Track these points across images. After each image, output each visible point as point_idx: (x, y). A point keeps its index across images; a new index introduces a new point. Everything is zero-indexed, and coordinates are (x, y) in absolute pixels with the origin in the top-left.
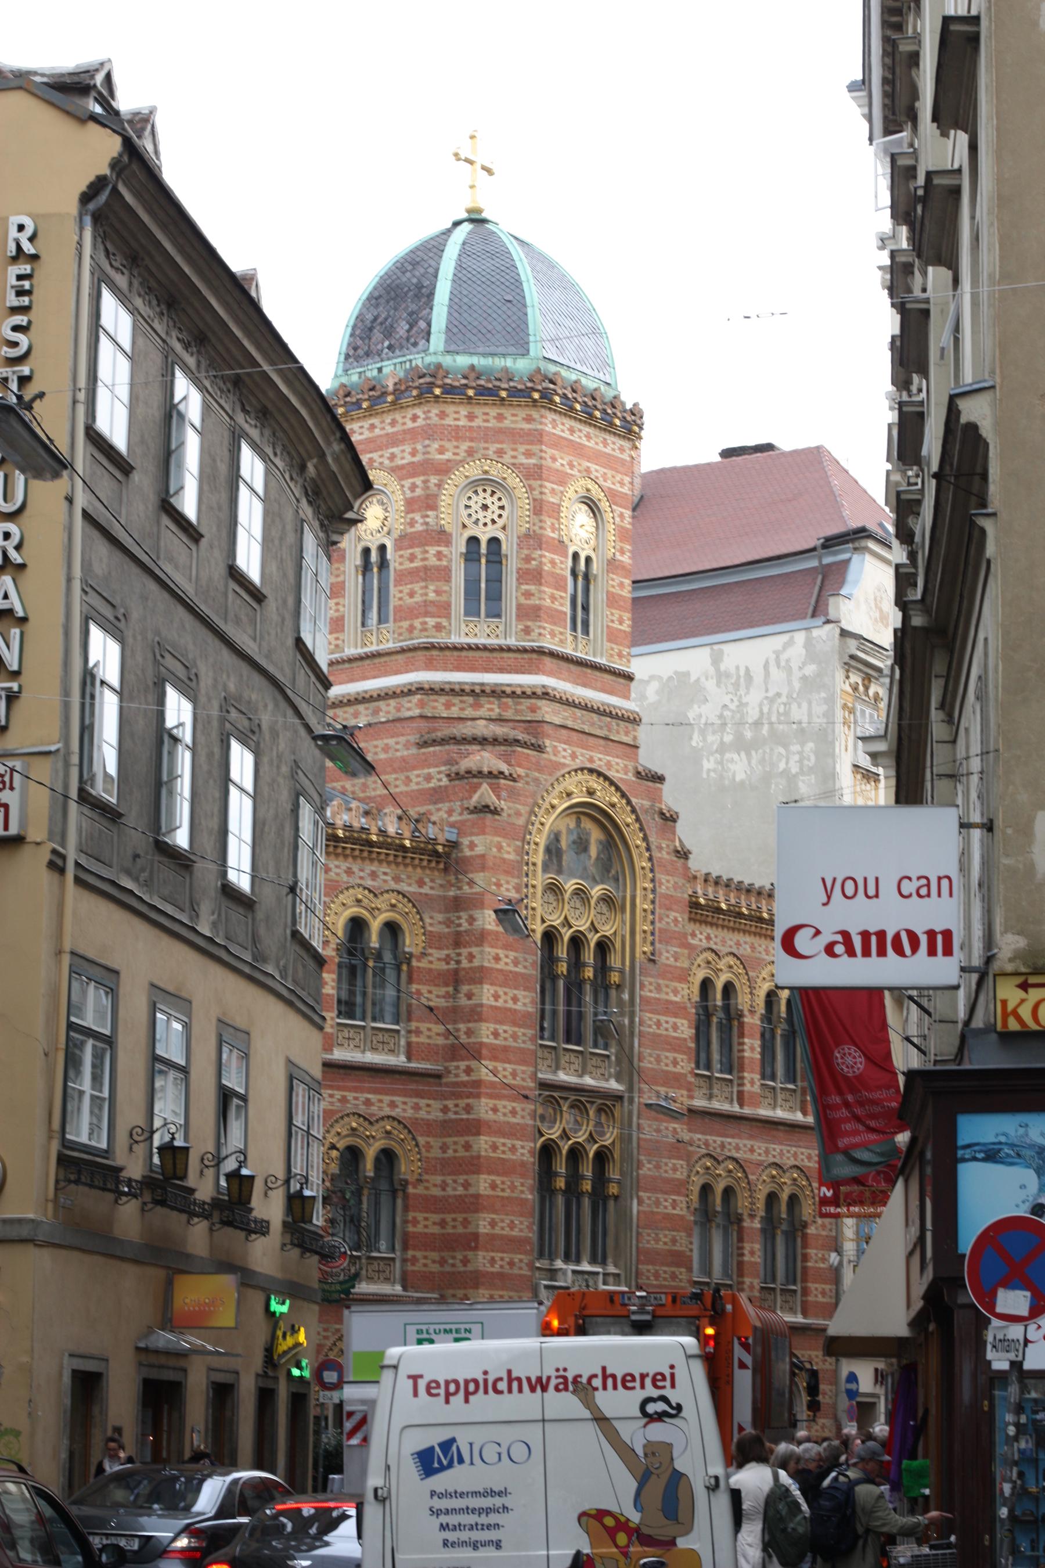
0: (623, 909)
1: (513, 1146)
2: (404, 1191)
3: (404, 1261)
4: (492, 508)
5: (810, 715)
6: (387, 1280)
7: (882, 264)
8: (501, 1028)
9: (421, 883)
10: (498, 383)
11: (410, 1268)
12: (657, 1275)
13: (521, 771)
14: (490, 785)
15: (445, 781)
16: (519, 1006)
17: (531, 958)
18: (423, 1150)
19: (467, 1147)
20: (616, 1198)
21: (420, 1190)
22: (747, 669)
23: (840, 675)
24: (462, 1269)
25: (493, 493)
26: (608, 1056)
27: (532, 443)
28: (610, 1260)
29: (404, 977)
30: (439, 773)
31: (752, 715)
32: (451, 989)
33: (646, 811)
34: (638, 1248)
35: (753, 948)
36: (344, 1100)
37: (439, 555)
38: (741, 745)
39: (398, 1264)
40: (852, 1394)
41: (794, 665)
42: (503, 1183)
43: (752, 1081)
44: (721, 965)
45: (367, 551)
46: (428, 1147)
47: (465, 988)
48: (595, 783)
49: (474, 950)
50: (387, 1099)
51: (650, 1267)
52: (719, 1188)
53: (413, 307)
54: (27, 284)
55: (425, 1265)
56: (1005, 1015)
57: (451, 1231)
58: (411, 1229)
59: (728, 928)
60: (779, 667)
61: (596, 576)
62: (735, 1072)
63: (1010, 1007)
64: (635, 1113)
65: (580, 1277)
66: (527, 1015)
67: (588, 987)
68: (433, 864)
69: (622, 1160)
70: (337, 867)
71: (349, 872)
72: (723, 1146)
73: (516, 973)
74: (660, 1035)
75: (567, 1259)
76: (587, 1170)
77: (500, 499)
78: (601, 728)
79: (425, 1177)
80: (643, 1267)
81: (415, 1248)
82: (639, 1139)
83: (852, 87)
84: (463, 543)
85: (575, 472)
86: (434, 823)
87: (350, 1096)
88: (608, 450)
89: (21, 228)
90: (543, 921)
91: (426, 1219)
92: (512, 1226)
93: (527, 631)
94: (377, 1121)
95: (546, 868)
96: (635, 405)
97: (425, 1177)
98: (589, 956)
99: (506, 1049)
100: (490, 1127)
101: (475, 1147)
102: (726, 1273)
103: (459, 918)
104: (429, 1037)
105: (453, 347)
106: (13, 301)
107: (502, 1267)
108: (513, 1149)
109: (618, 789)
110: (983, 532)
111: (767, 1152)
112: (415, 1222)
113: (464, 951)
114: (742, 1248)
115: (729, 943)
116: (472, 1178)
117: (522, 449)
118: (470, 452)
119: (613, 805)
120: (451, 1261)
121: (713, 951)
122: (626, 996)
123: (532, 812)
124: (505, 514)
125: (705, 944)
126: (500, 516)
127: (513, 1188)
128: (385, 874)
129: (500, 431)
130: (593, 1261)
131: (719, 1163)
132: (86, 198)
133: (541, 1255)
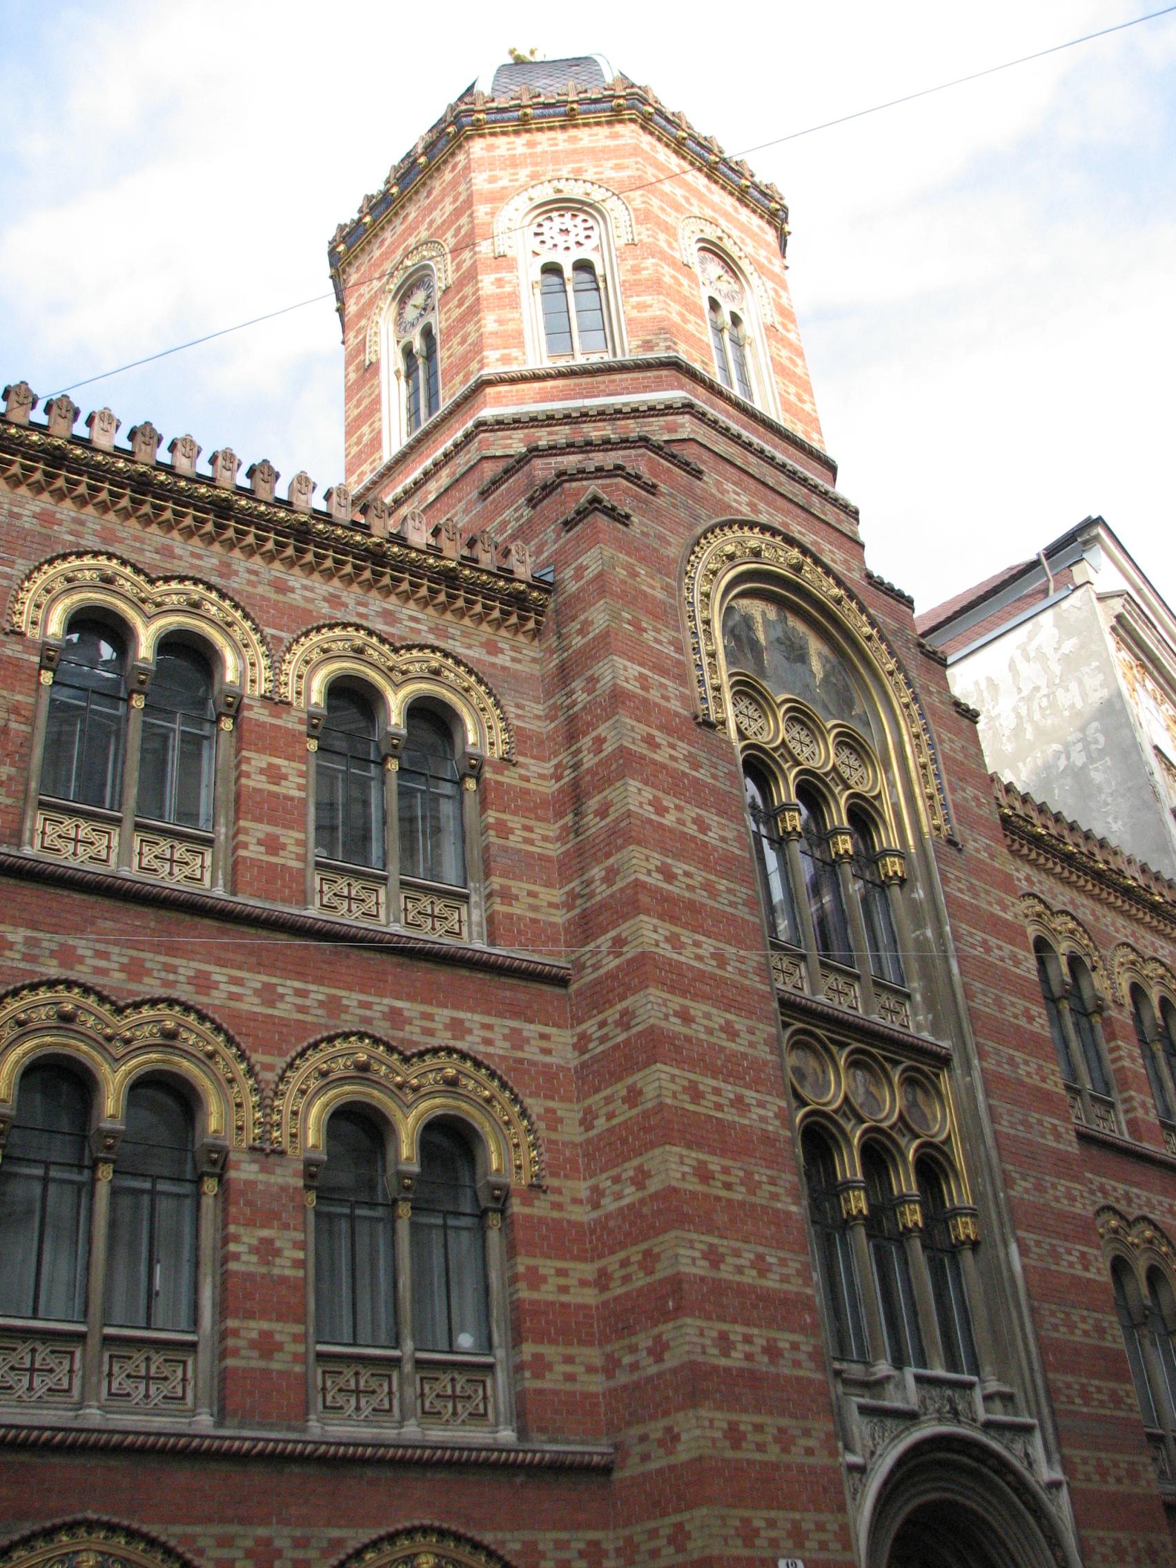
0: (887, 767)
2: (502, 1212)
3: (519, 1368)
4: (573, 231)
5: (1084, 695)
6: (478, 1417)
8: (679, 868)
9: (492, 648)
11: (530, 1383)
12: (1085, 1394)
13: (663, 488)
14: (603, 487)
15: (527, 512)
16: (712, 837)
17: (723, 768)
18: (541, 1125)
19: (634, 1096)
20: (975, 1245)
21: (541, 1208)
22: (990, 680)
23: (1110, 641)
24: (653, 1370)
27: (623, 157)
28: (987, 1370)
29: (471, 801)
32: (569, 819)
33: (894, 633)
34: (1038, 1338)
36: (333, 1006)
37: (499, 282)
41: (1048, 651)
45: (408, 353)
46: (553, 1121)
47: (593, 803)
49: (602, 730)
50: (444, 1015)
51: (1070, 1378)
52: (1141, 1267)
55: (570, 1377)
57: (620, 1291)
58: (525, 1293)
60: (1028, 660)
65: (935, 1392)
66: (729, 858)
68: (514, 619)
69: (973, 1172)
70: (305, 587)
71: (333, 600)
72: (1129, 1201)
73: (696, 780)
74: (991, 965)
76: (905, 1182)
79: (549, 1181)
80: (1059, 1379)
81: (541, 1337)
82: (996, 1132)
87: (351, 999)
90: (742, 735)
91: (561, 1273)
92: (761, 1266)
94: (421, 1055)
95: (732, 659)
99: (692, 907)
100: (678, 1050)
101: (650, 1091)
103: (569, 695)
108: (738, 1103)
112: (535, 1279)
113: (586, 742)
118: (534, 176)
120: (627, 1360)
122: (920, 894)
126: (588, 237)
127: (752, 1186)
128: (413, 619)
129: (575, 152)
133: (843, 1355)
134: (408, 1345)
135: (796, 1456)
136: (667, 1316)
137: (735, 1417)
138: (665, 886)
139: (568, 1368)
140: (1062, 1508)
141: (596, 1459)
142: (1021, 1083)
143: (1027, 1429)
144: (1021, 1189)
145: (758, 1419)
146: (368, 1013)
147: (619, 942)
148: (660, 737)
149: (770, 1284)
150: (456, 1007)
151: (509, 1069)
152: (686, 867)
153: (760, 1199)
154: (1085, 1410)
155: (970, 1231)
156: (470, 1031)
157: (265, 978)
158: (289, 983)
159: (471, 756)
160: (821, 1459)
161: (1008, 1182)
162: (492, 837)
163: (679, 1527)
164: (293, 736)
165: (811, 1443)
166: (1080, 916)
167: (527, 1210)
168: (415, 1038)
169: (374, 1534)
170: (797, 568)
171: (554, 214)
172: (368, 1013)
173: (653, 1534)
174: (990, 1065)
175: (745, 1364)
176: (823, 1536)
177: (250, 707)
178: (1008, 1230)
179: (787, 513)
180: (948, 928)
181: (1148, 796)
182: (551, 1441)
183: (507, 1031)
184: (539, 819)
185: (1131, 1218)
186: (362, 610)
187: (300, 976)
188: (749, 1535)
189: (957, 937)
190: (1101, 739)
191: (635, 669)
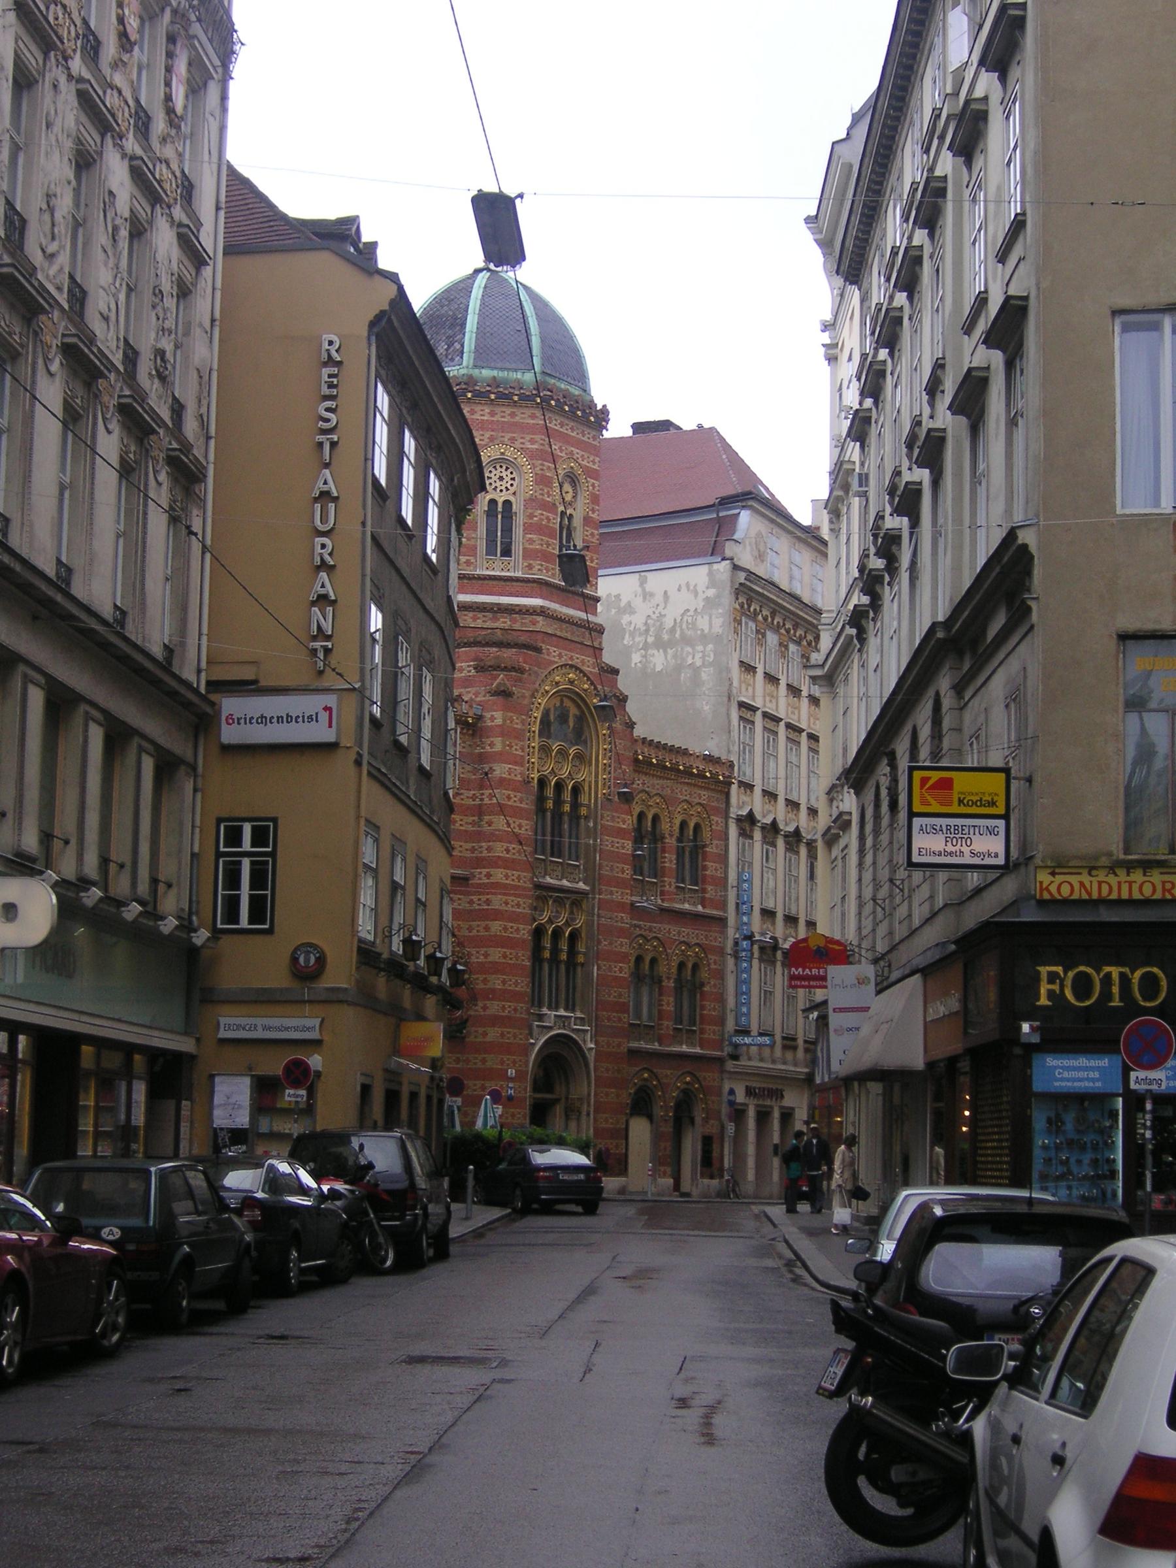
0: (590, 765)
1: (518, 928)
7: (825, 343)
10: (512, 391)
12: (609, 1019)
13: (527, 667)
16: (522, 831)
19: (487, 928)
20: (582, 965)
25: (507, 469)
28: (577, 1008)
30: (469, 666)
31: (668, 623)
32: (476, 818)
38: (660, 644)
40: (732, 1103)
41: (700, 589)
43: (670, 884)
53: (450, 332)
54: (335, 381)
56: (1041, 890)
59: (657, 776)
61: (575, 528)
63: (1044, 886)
64: (596, 906)
67: (566, 818)
68: (465, 731)
75: (550, 1008)
77: (511, 473)
78: (578, 636)
82: (598, 924)
83: (808, 220)
84: (486, 503)
85: (563, 454)
86: (466, 702)
88: (585, 439)
89: (331, 343)
93: (530, 567)
96: (604, 406)
98: (567, 796)
99: (514, 860)
101: (493, 929)
102: (650, 1018)
104: (461, 852)
105: (479, 363)
106: (325, 391)
109: (589, 679)
110: (1029, 609)
111: (679, 934)
114: (662, 1000)
116: (491, 950)
117: (528, 437)
118: (492, 439)
119: (585, 690)
121: (646, 792)
122: (591, 824)
123: (533, 696)
124: (515, 484)
129: (515, 424)
130: (566, 1009)
131: (648, 941)
132: (372, 324)
136: (489, 999)
140: (591, 1057)
142: (613, 901)
143: (587, 1031)
147: (488, 876)
161: (599, 942)
163: (484, 1058)
173: (476, 1058)
181: (726, 699)
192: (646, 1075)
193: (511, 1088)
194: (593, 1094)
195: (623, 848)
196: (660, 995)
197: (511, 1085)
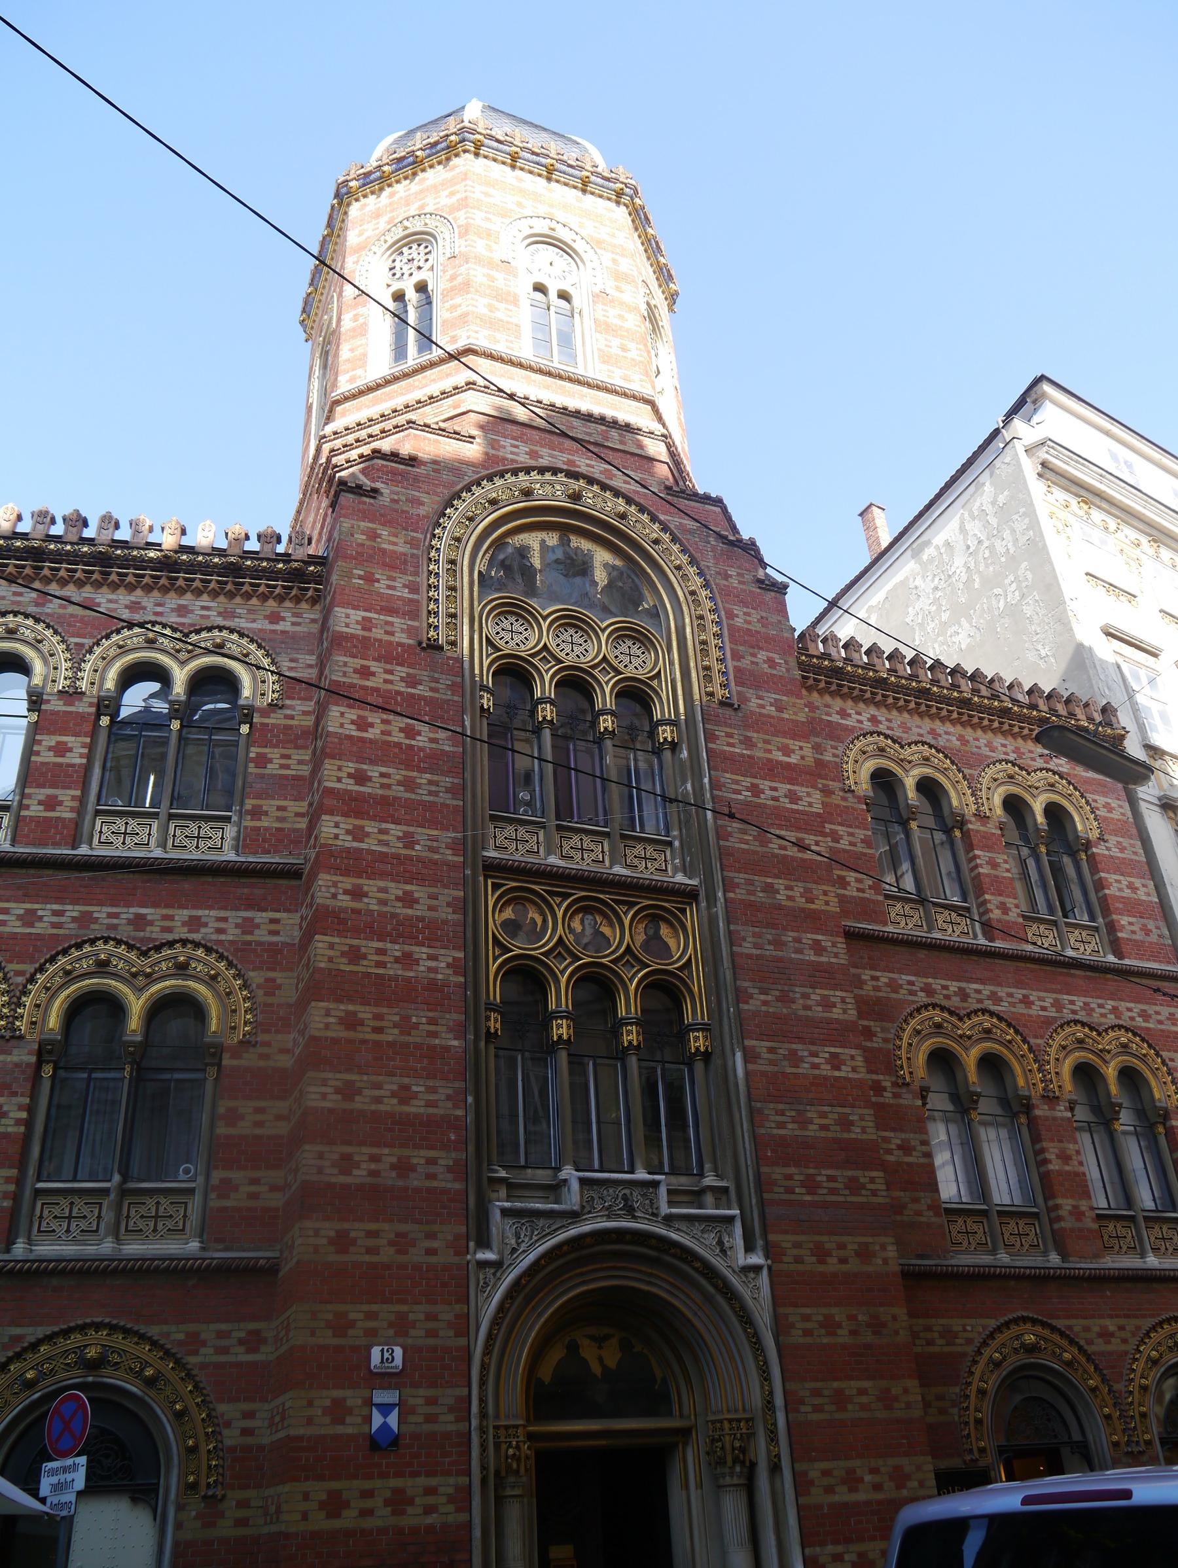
1: (407, 956)
2: (219, 1065)
9: (275, 618)
12: (811, 1185)
20: (707, 1056)
21: (249, 1059)
26: (670, 844)
28: (707, 1166)
33: (690, 532)
34: (755, 1137)
35: (961, 738)
36: (85, 920)
37: (355, 318)
39: (198, 1197)
41: (989, 508)
42: (378, 1017)
44: (906, 753)
46: (271, 987)
48: (576, 485)
51: (792, 1170)
55: (253, 1196)
58: (222, 1130)
62: (971, 897)
72: (963, 995)
73: (412, 695)
82: (733, 955)
87: (101, 912)
97: (266, 1037)
99: (384, 801)
100: (343, 922)
107: (374, 1173)
115: (915, 730)
119: (623, 516)
122: (685, 754)
125: (867, 726)
126: (427, 260)
127: (406, 1026)
128: (203, 608)
134: (117, 1178)
135: (416, 1255)
137: (346, 1226)
138: (357, 788)
139: (253, 1189)
141: (262, 1262)
142: (780, 907)
143: (730, 1220)
144: (756, 1002)
145: (373, 1226)
146: (115, 921)
148: (374, 666)
149: (413, 1110)
150: (195, 907)
151: (237, 950)
152: (384, 770)
153: (415, 1038)
154: (808, 1198)
155: (701, 1043)
156: (206, 925)
157: (28, 906)
158: (48, 906)
159: (243, 707)
160: (446, 1257)
161: (741, 996)
162: (252, 768)
164: (82, 716)
165: (435, 1244)
166: (941, 742)
167: (235, 1062)
168: (154, 936)
169: (49, 1330)
170: (576, 497)
171: (405, 250)
172: (115, 921)
174: (739, 894)
175: (369, 1180)
176: (431, 1325)
177: (48, 701)
178: (735, 1041)
179: (570, 451)
180: (706, 780)
182: (226, 1249)
183: (239, 921)
184: (297, 747)
185: (962, 1013)
186: (159, 609)
187: (59, 900)
188: (341, 1326)
189: (715, 784)
190: (1030, 576)
191: (357, 615)
192: (1030, 1338)
193: (385, 1409)
194: (779, 1401)
195: (793, 797)
196: (1036, 1138)
197: (380, 1397)
